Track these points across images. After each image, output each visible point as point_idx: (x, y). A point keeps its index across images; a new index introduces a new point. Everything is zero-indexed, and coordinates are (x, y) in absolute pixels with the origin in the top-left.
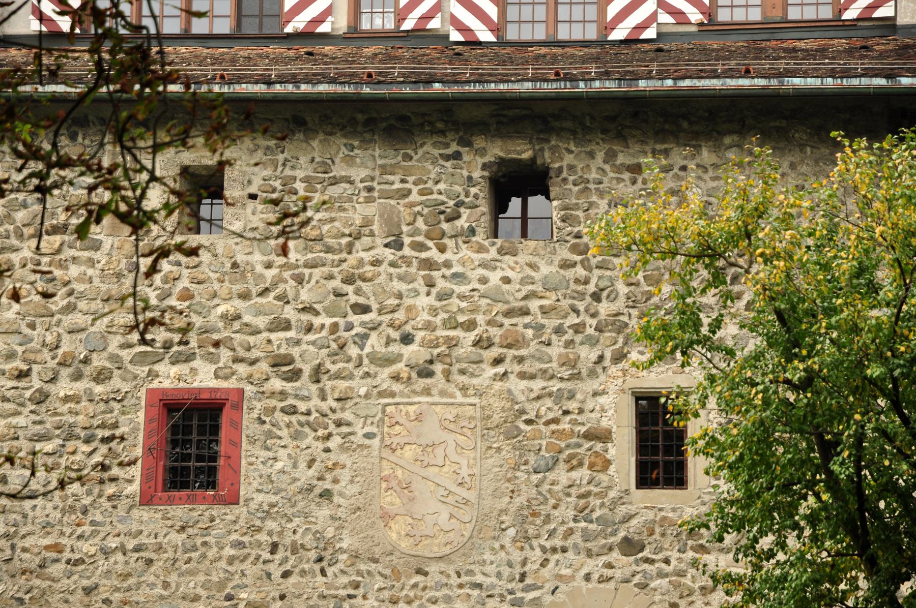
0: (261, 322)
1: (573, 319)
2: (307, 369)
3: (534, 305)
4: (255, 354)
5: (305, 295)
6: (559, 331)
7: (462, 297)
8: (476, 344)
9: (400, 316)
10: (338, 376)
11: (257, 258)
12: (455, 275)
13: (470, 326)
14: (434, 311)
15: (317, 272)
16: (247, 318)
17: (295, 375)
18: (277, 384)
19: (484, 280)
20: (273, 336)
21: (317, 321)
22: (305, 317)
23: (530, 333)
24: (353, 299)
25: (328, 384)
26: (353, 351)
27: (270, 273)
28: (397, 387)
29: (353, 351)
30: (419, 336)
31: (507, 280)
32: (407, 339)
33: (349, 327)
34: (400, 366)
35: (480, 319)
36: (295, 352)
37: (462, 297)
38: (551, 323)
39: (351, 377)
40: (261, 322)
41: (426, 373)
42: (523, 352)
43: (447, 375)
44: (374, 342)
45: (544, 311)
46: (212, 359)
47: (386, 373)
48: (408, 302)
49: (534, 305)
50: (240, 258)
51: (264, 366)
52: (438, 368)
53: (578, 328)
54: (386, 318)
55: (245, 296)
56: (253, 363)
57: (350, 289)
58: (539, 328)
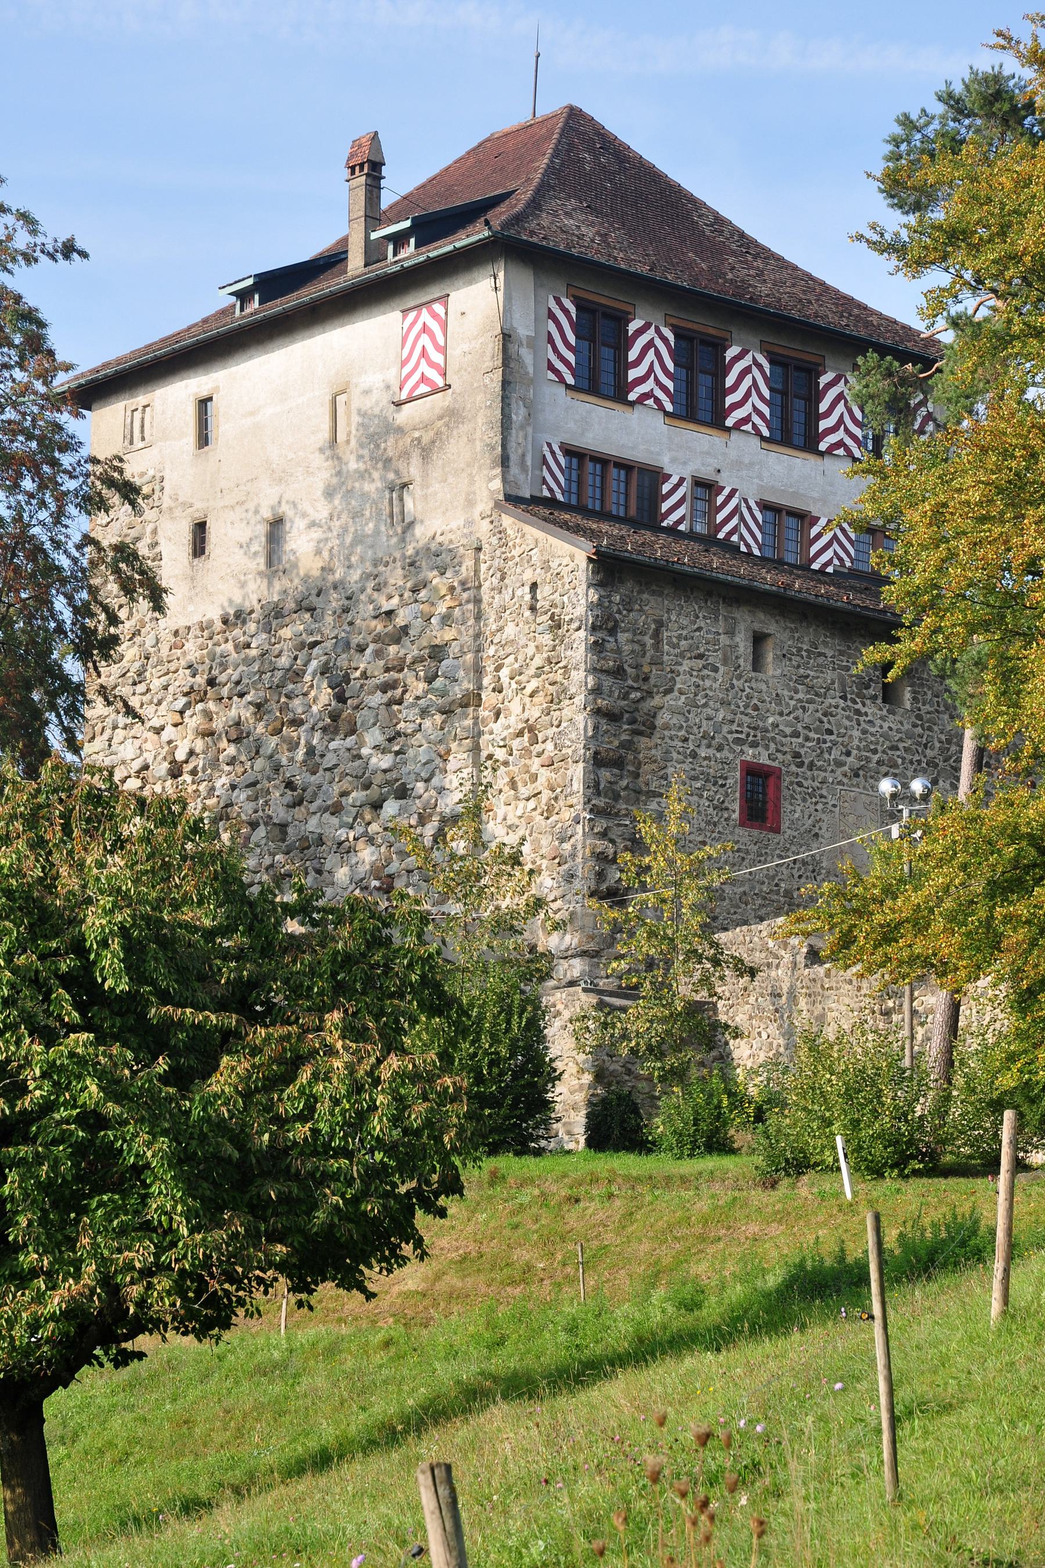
0: (788, 731)
1: (917, 757)
2: (807, 761)
3: (901, 745)
4: (785, 749)
6: (911, 762)
7: (872, 735)
8: (878, 763)
9: (846, 739)
10: (819, 769)
11: (786, 693)
12: (870, 722)
13: (875, 752)
14: (860, 740)
16: (781, 727)
17: (800, 765)
18: (793, 768)
19: (881, 727)
20: (793, 740)
21: (812, 735)
22: (806, 732)
23: (900, 761)
24: (827, 726)
25: (816, 773)
26: (826, 756)
27: (792, 703)
28: (845, 780)
29: (826, 756)
30: (854, 752)
31: (890, 729)
32: (848, 754)
33: (825, 742)
34: (846, 768)
35: (879, 748)
36: (802, 751)
37: (872, 735)
38: (909, 757)
39: (825, 771)
40: (788, 731)
41: (857, 775)
42: (897, 771)
43: (865, 777)
44: (835, 753)
45: (906, 749)
46: (767, 747)
47: (839, 771)
48: (849, 733)
49: (901, 745)
50: (779, 691)
51: (789, 757)
52: (861, 773)
53: (919, 762)
54: (840, 740)
55: (781, 714)
56: (785, 753)
57: (825, 719)
58: (903, 759)
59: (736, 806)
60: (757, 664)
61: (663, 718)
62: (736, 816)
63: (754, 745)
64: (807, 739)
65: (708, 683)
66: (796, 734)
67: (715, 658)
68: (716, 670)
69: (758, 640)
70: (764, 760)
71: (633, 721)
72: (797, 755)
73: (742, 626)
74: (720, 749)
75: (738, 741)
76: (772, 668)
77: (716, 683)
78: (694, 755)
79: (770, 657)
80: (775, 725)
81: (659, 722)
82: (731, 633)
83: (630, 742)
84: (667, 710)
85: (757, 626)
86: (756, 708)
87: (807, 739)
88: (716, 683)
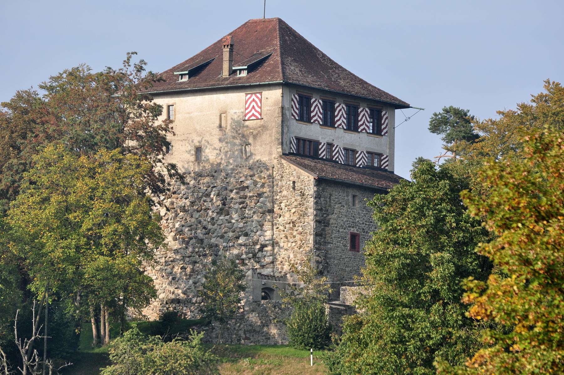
0: (361, 223)
5: (366, 219)
15: (367, 215)
21: (367, 223)
40: (361, 223)
59: (349, 245)
60: (354, 205)
61: (332, 221)
62: (349, 248)
63: (353, 227)
64: (366, 225)
65: (342, 211)
66: (363, 223)
67: (344, 203)
68: (344, 207)
69: (354, 196)
70: (356, 232)
71: (324, 223)
72: (363, 229)
73: (350, 194)
74: (345, 229)
75: (349, 227)
76: (357, 206)
77: (344, 211)
78: (339, 231)
79: (357, 202)
80: (358, 221)
81: (330, 223)
82: (348, 196)
83: (324, 229)
84: (332, 218)
85: (354, 193)
86: (354, 217)
87: (366, 225)
88: (344, 211)
